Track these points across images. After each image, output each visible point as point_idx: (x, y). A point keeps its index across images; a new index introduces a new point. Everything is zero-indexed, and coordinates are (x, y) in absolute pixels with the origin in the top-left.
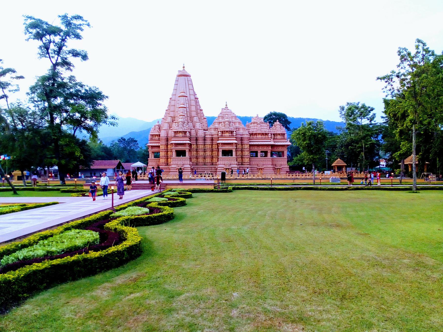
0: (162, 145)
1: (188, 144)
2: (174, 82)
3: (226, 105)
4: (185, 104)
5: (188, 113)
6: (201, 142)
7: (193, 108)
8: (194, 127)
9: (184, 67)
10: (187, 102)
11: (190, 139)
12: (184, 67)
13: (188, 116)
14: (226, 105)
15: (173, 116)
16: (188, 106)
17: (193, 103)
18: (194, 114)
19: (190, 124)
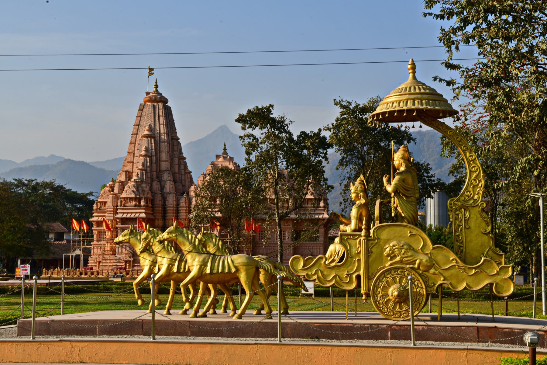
0: (109, 220)
1: (143, 219)
2: (136, 112)
3: (225, 149)
4: (150, 150)
5: (154, 165)
6: (170, 215)
7: (164, 156)
8: (162, 188)
9: (156, 86)
10: (153, 148)
11: (153, 211)
12: (156, 86)
13: (154, 169)
14: (225, 149)
15: (130, 170)
16: (154, 154)
17: (164, 147)
18: (165, 165)
19: (156, 185)
